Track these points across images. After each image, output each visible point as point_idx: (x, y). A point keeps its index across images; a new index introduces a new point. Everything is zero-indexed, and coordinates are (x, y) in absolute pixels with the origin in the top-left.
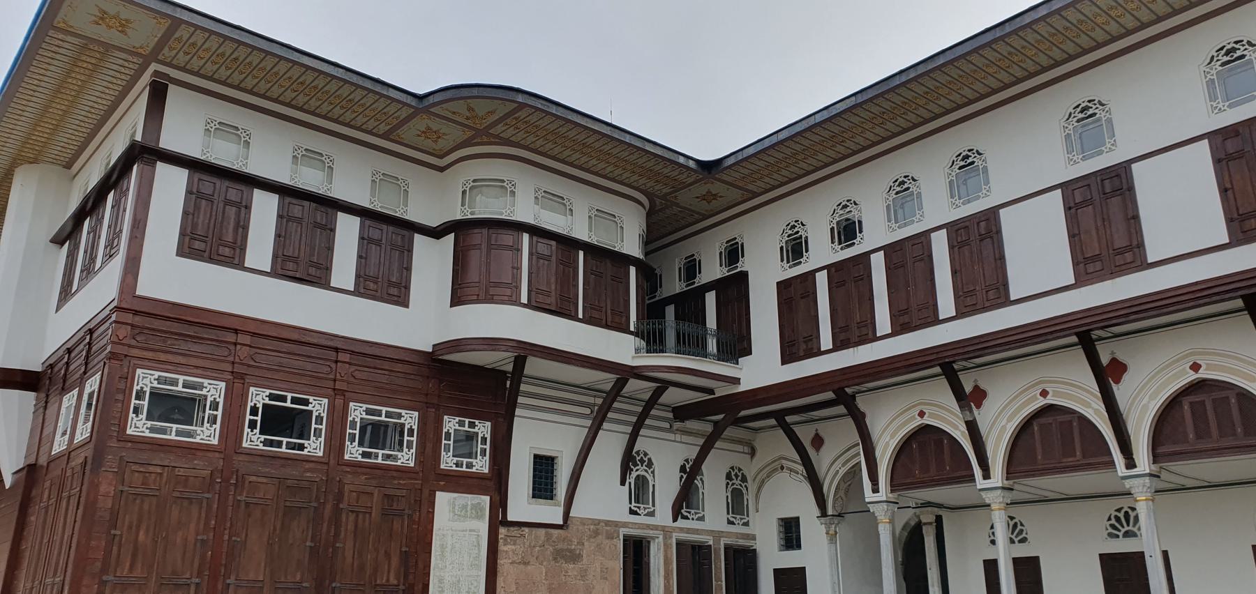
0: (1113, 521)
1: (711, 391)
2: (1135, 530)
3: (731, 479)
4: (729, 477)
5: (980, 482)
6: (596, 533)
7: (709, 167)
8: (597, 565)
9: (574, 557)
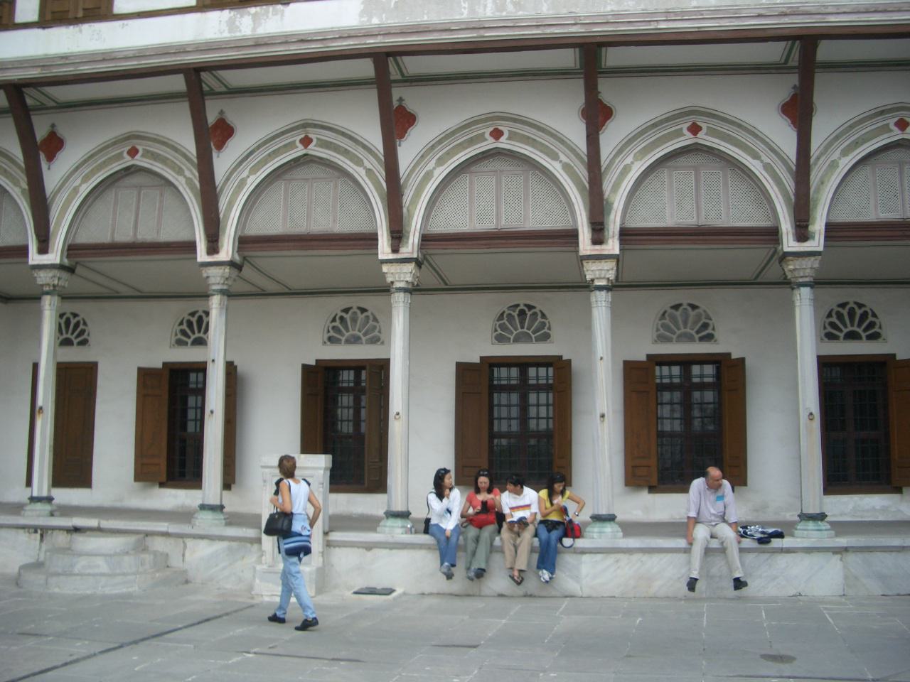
0: (185, 327)
2: (205, 337)
5: (35, 258)
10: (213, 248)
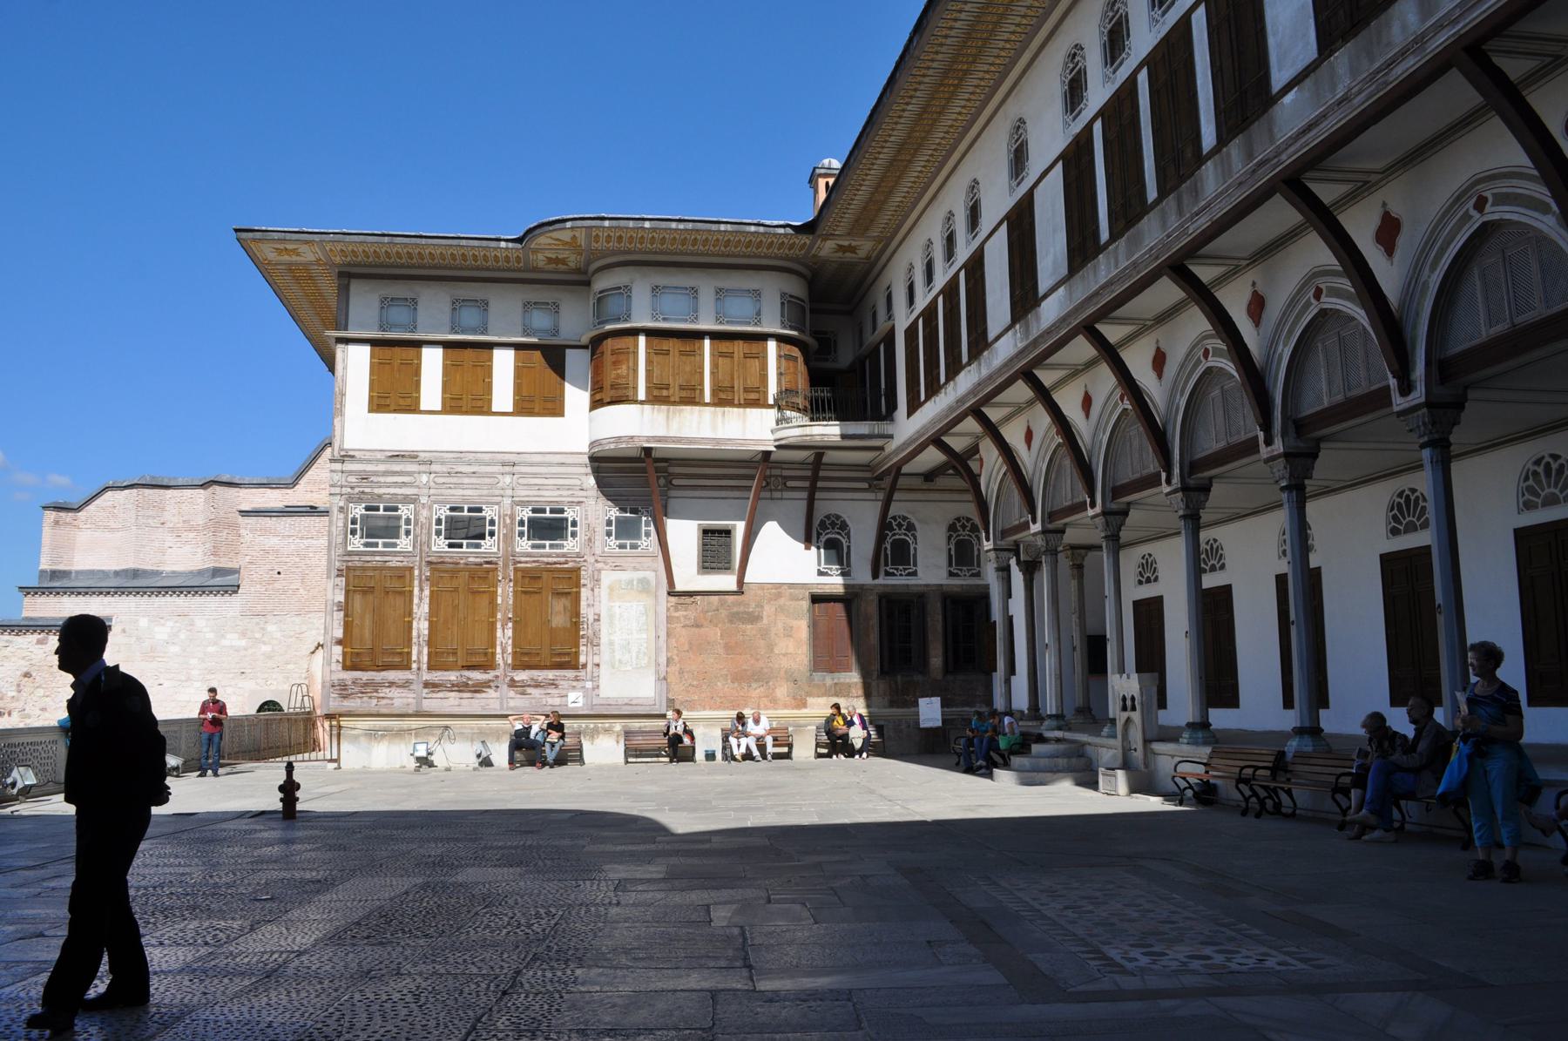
1: (881, 448)
3: (956, 530)
4: (952, 528)
6: (779, 595)
7: (808, 228)
8: (780, 625)
9: (754, 618)
10: (1093, 505)
